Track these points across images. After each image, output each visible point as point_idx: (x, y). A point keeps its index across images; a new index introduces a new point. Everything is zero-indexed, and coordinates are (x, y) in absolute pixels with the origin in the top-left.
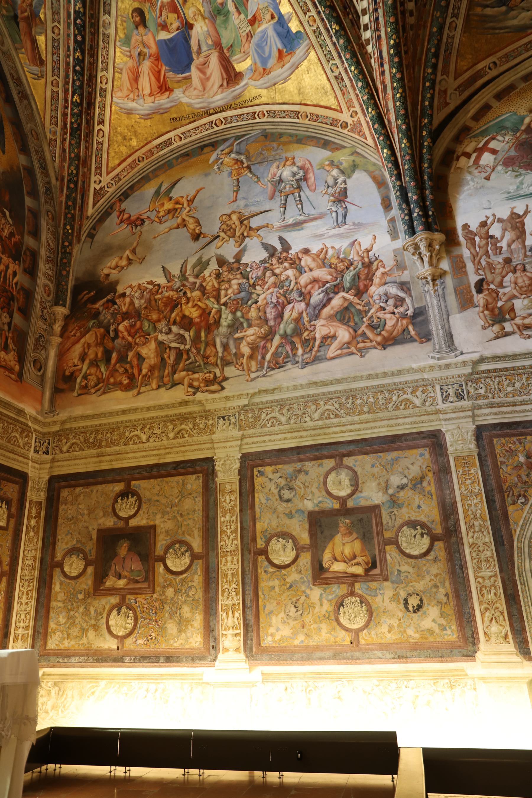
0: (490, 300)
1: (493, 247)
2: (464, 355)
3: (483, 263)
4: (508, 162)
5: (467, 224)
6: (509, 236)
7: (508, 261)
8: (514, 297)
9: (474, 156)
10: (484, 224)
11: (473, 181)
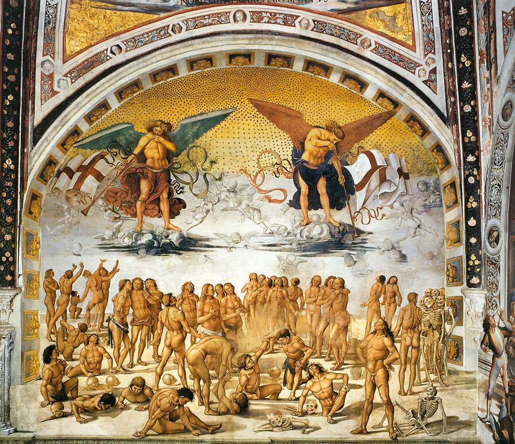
0: (56, 373)
1: (72, 307)
2: (18, 433)
3: (58, 326)
4: (111, 197)
5: (51, 270)
6: (92, 297)
7: (83, 328)
8: (82, 374)
9: (77, 175)
10: (69, 275)
11: (69, 213)
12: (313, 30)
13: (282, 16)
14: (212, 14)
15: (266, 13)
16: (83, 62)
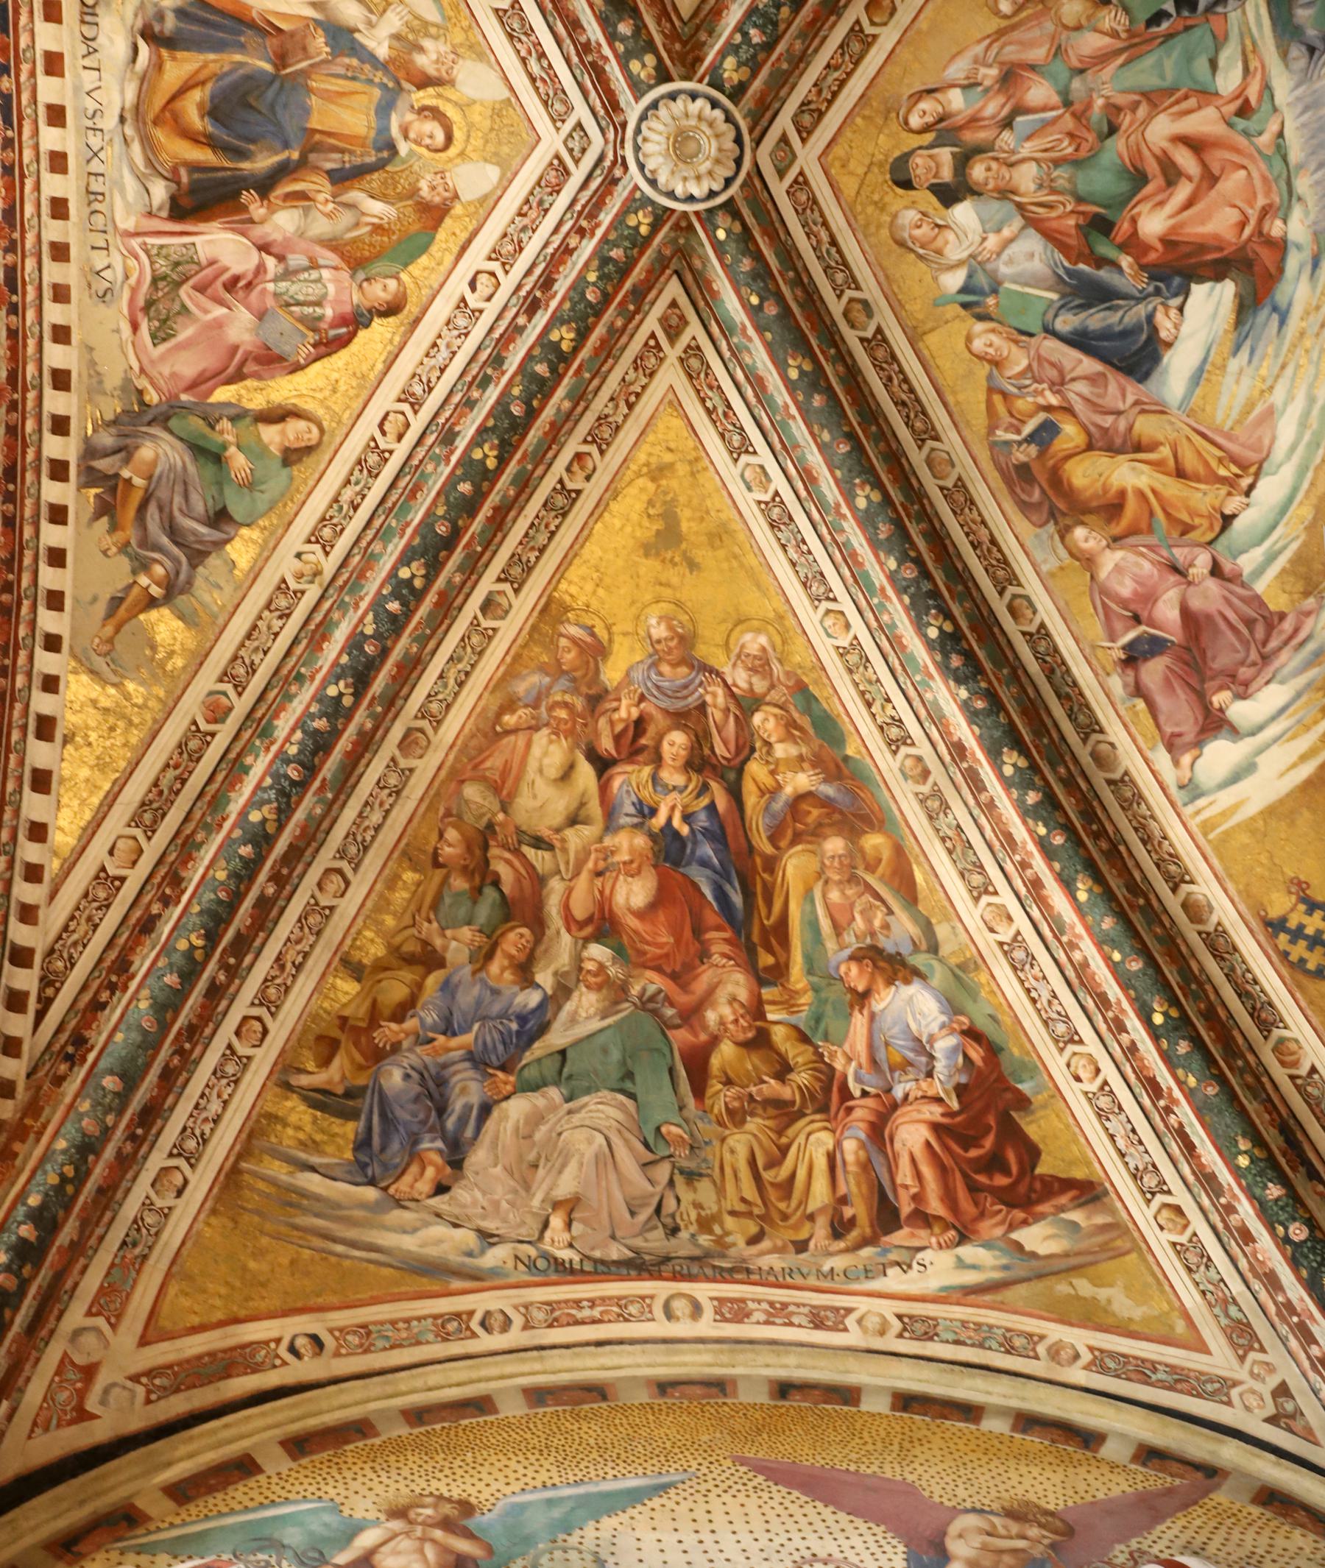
12: (900, 1336)
13: (806, 1310)
14: (603, 1299)
15: (759, 1302)
16: (199, 1357)
